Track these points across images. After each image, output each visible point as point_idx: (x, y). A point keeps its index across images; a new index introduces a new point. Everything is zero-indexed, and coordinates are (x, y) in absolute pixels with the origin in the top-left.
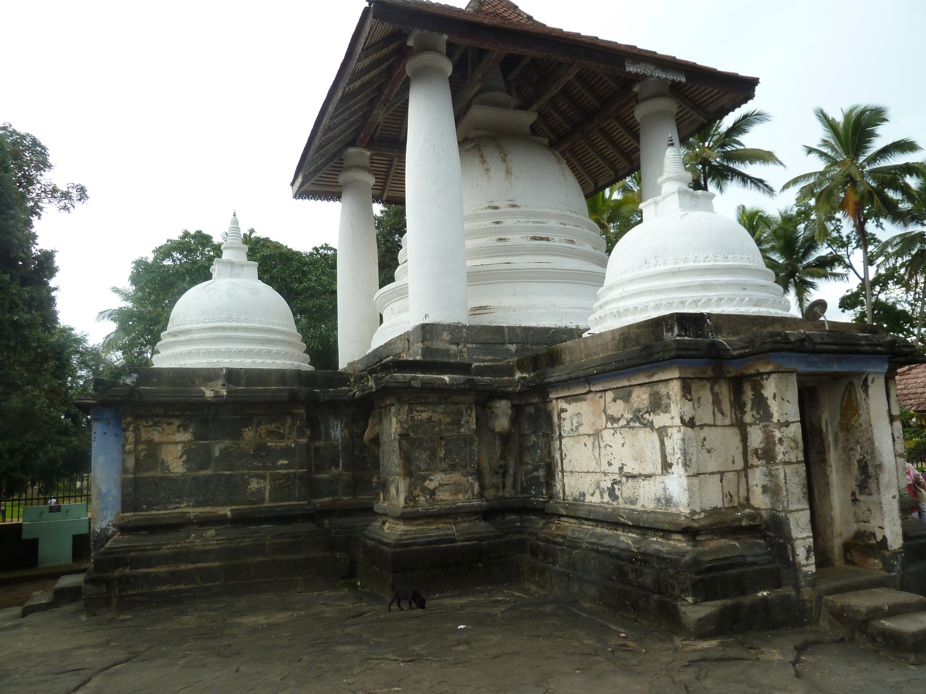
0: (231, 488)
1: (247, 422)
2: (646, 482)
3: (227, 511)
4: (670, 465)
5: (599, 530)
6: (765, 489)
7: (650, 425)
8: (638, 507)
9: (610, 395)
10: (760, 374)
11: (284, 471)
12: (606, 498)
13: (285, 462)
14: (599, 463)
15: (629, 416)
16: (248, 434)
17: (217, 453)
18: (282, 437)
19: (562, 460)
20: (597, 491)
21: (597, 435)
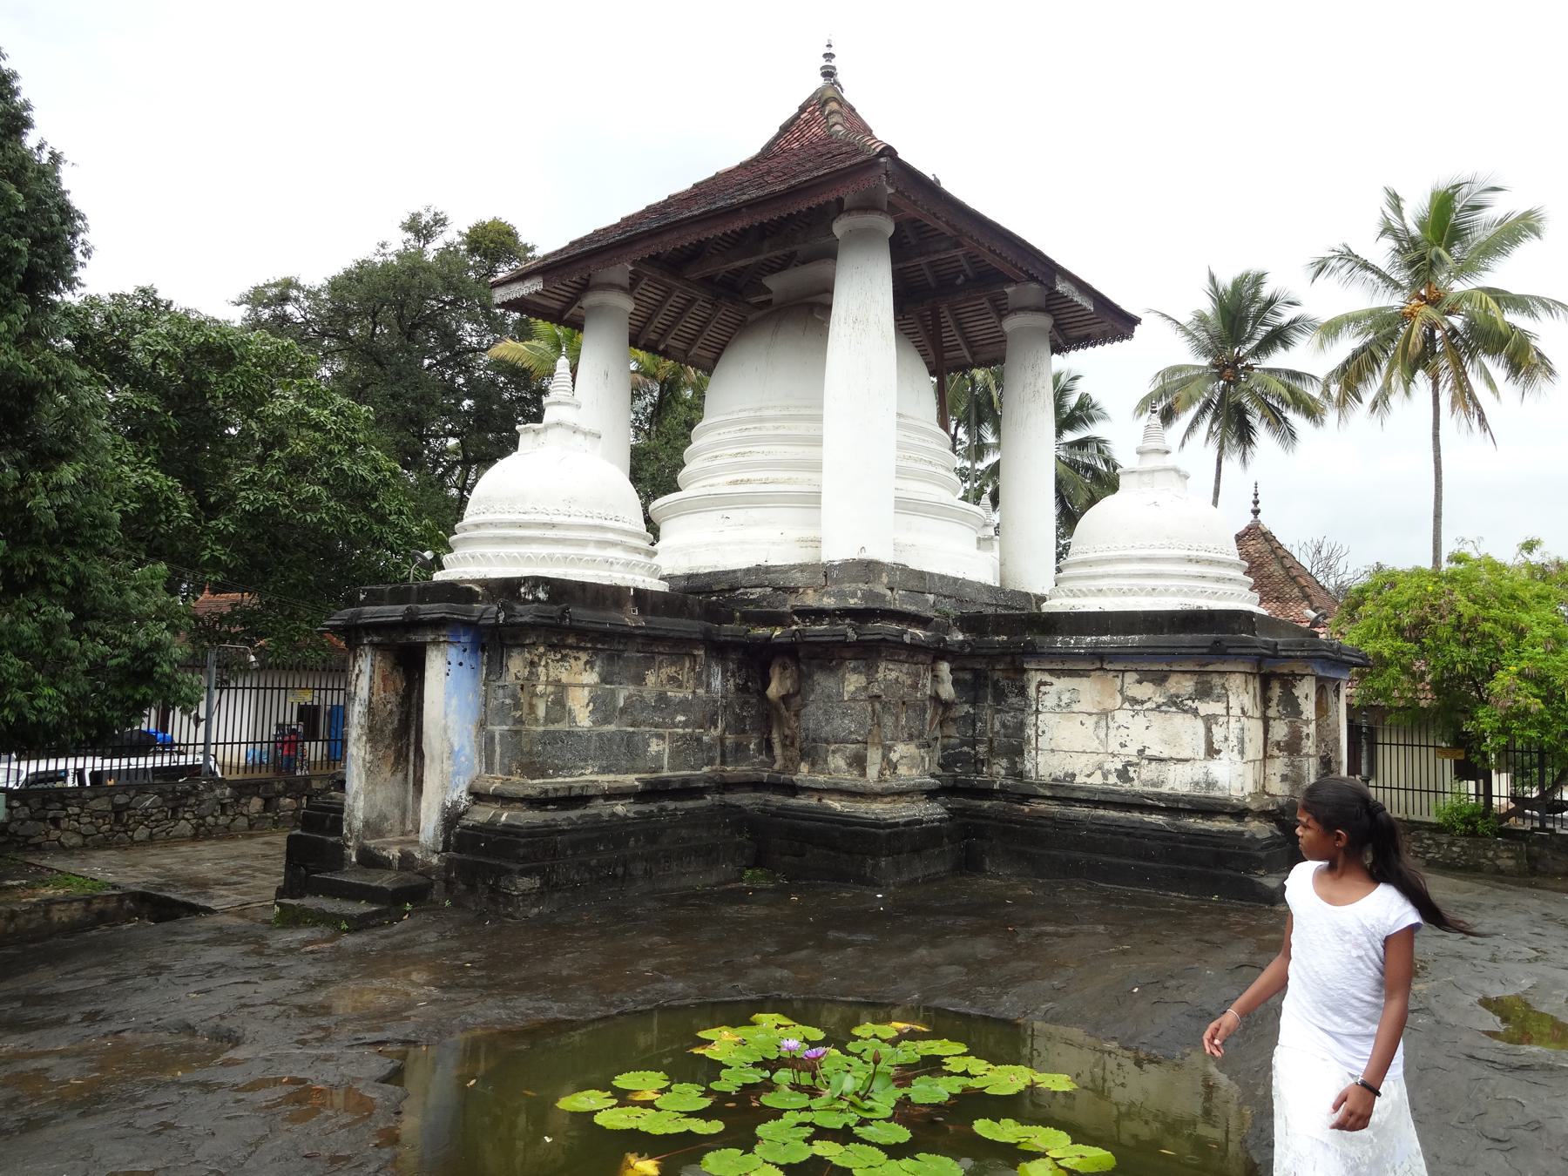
0: (631, 748)
1: (649, 662)
2: (1179, 766)
3: (631, 780)
4: (1218, 752)
5: (1101, 812)
6: (1284, 778)
7: (1195, 712)
8: (1165, 789)
9: (1130, 678)
10: (1294, 675)
11: (680, 731)
12: (1113, 779)
13: (683, 718)
15: (1162, 700)
16: (651, 678)
18: (680, 686)
19: (1037, 736)
20: (1099, 773)
21: (1105, 714)
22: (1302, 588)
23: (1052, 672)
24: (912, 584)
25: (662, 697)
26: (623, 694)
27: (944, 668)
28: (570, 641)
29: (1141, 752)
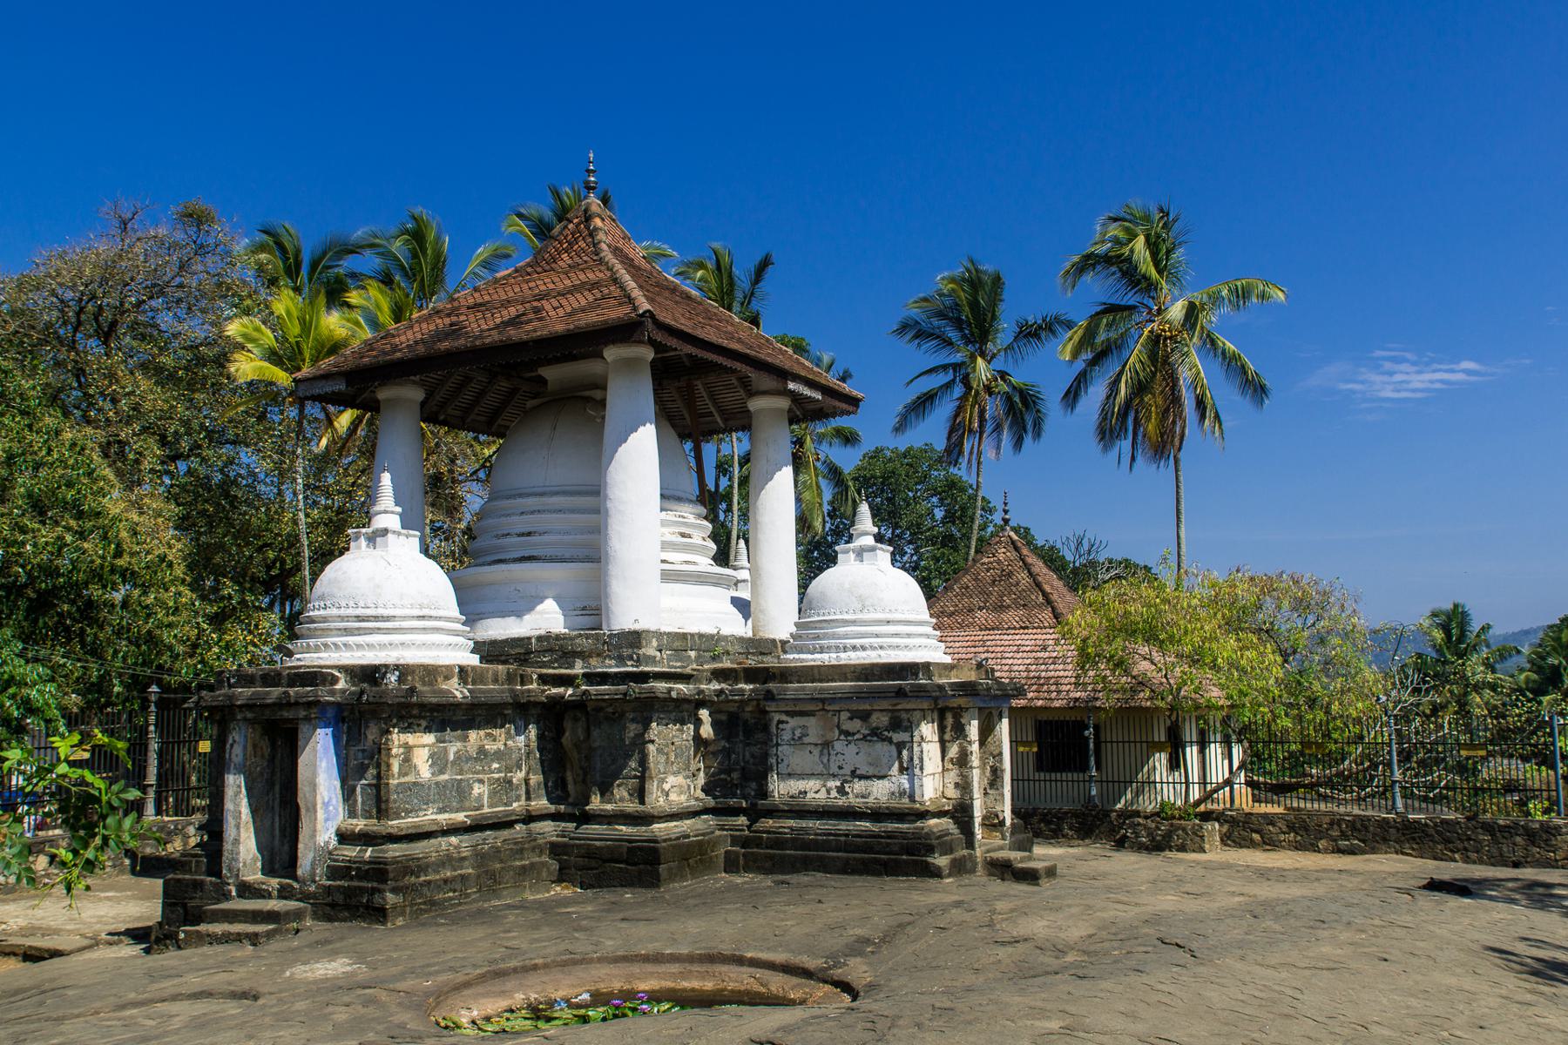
0: (461, 791)
3: (460, 817)
6: (957, 785)
7: (890, 740)
8: (871, 800)
12: (834, 794)
14: (827, 766)
17: (451, 757)
21: (826, 745)
22: (1045, 594)
23: (787, 713)
24: (677, 644)
25: (482, 750)
26: (453, 749)
27: (704, 714)
28: (415, 712)
29: (853, 772)
